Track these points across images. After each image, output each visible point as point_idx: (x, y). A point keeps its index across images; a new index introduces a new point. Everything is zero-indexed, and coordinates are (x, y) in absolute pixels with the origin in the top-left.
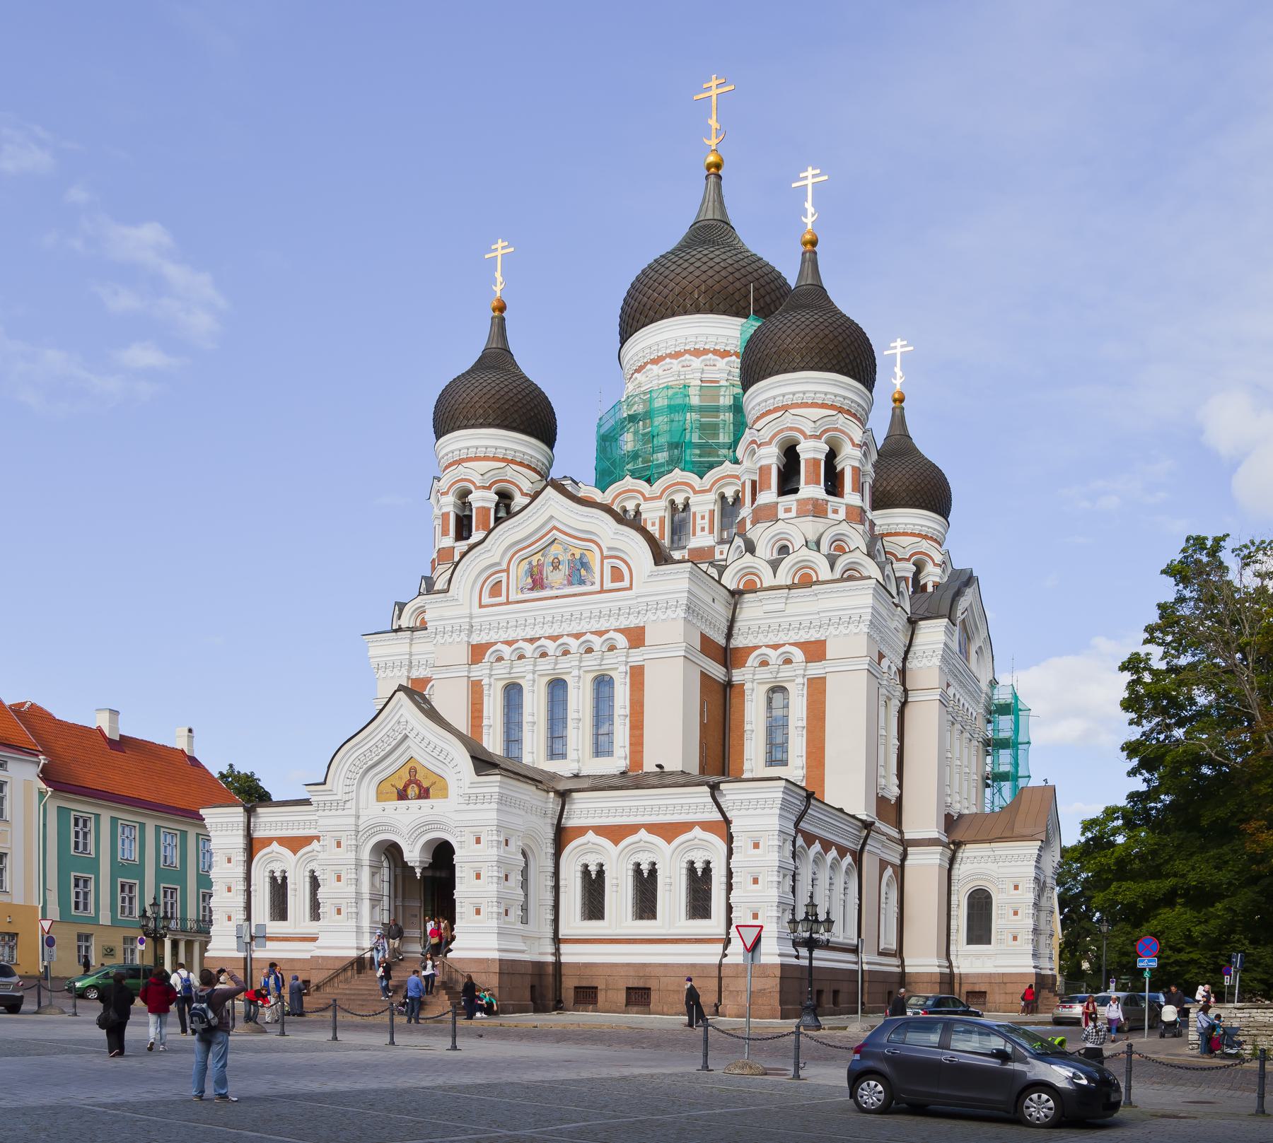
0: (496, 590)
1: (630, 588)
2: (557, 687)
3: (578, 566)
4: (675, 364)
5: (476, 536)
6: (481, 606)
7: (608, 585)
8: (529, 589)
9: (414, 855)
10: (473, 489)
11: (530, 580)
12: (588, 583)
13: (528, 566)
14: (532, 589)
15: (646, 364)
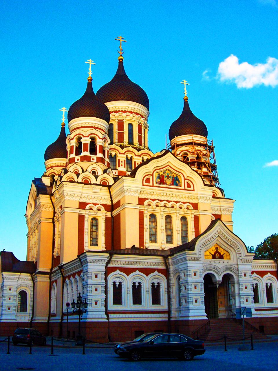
0: (148, 181)
1: (194, 191)
2: (168, 218)
3: (176, 180)
4: (131, 115)
5: (84, 154)
6: (143, 185)
7: (186, 188)
8: (159, 183)
9: (219, 278)
10: (97, 138)
11: (159, 180)
12: (179, 186)
13: (158, 175)
14: (160, 183)
15: (119, 111)
